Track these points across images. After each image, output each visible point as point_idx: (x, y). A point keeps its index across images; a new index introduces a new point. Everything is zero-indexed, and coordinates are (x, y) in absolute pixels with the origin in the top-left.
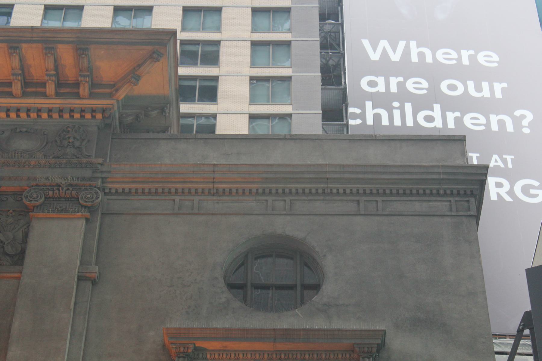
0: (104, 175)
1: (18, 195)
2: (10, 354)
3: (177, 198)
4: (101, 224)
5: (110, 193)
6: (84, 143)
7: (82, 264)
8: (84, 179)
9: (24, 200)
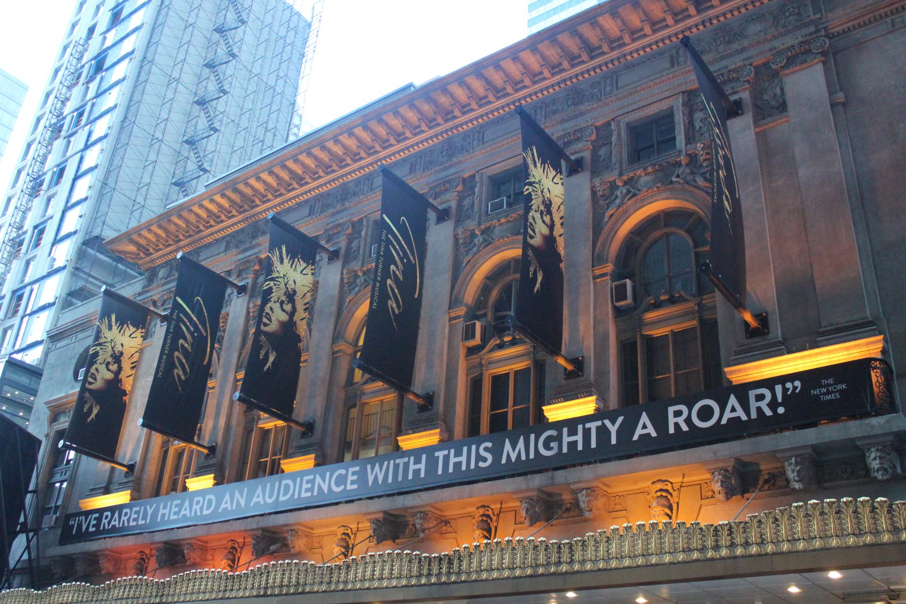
0: (825, 25)
1: (766, 65)
2: (800, 174)
3: (888, 20)
4: (835, 61)
5: (834, 36)
6: (802, 8)
7: (831, 94)
8: (811, 34)
9: (773, 66)
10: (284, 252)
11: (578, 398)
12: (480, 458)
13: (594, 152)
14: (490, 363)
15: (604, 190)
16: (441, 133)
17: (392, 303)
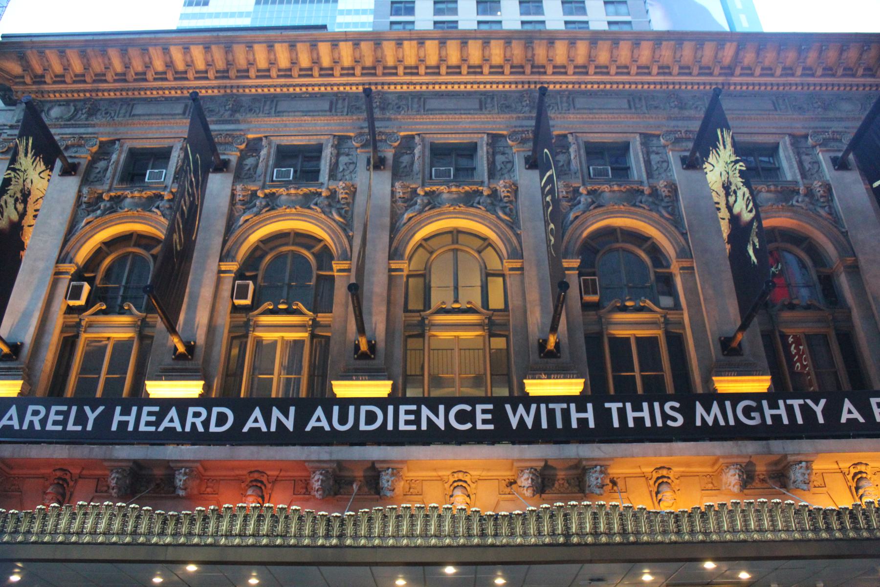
10: (30, 145)
11: (752, 375)
12: (665, 417)
13: (241, 159)
14: (258, 326)
15: (244, 196)
16: (523, 83)
17: (175, 237)
